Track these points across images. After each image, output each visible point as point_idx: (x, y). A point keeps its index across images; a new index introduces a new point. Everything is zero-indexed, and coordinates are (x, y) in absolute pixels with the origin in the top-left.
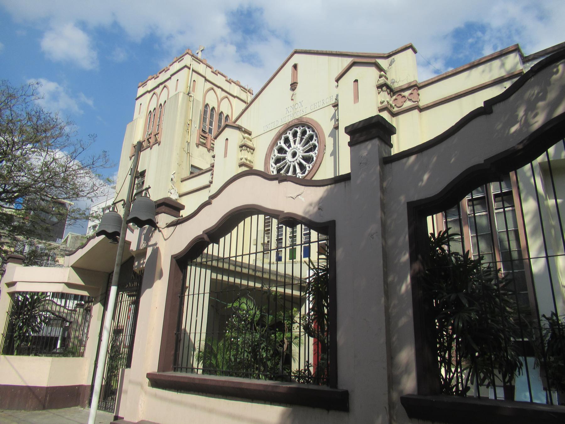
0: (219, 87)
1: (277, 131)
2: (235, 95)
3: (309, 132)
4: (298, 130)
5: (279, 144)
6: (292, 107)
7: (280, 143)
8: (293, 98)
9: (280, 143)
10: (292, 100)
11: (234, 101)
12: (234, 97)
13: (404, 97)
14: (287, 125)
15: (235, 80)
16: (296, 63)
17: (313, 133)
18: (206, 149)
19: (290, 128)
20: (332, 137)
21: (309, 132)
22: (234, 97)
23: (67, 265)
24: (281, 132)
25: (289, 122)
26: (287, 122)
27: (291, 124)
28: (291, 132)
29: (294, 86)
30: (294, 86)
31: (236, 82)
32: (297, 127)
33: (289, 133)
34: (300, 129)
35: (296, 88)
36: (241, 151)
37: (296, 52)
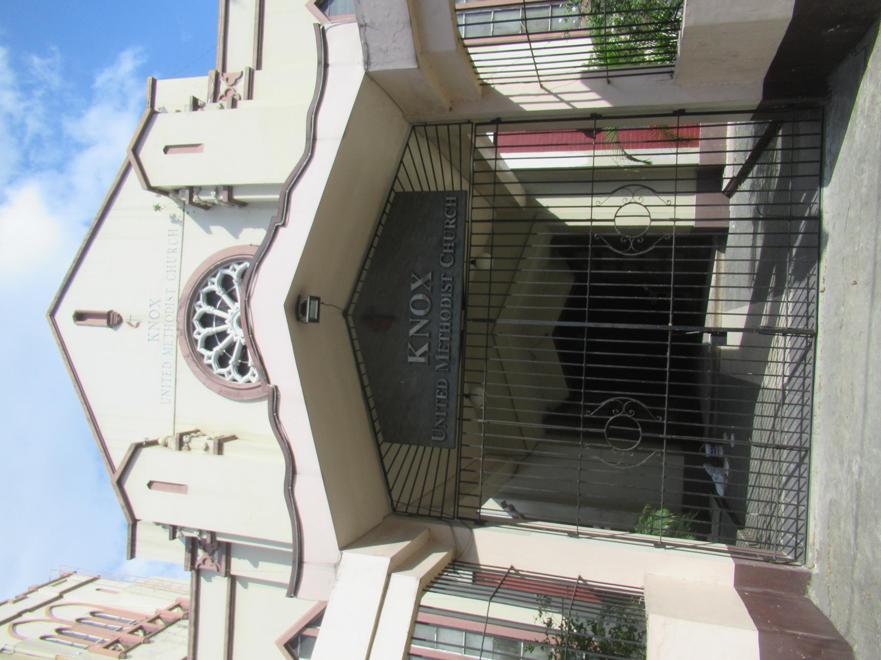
0: (20, 614)
1: (183, 364)
2: (57, 594)
3: (214, 286)
4: (199, 311)
5: (211, 362)
6: (151, 325)
7: (210, 358)
8: (134, 323)
9: (210, 358)
10: (138, 325)
11: (67, 598)
12: (60, 596)
13: (227, 91)
14: (181, 334)
15: (26, 590)
16: (72, 313)
17: (218, 275)
18: (143, 646)
19: (190, 328)
20: (240, 231)
21: (214, 286)
22: (60, 596)
23: (332, 569)
24: (188, 350)
25: (178, 329)
26: (175, 332)
27: (183, 326)
28: (199, 328)
29: (112, 320)
30: (112, 320)
31: (30, 590)
32: (195, 312)
33: (199, 334)
34: (200, 306)
35: (119, 315)
36: (189, 449)
37: (52, 314)
